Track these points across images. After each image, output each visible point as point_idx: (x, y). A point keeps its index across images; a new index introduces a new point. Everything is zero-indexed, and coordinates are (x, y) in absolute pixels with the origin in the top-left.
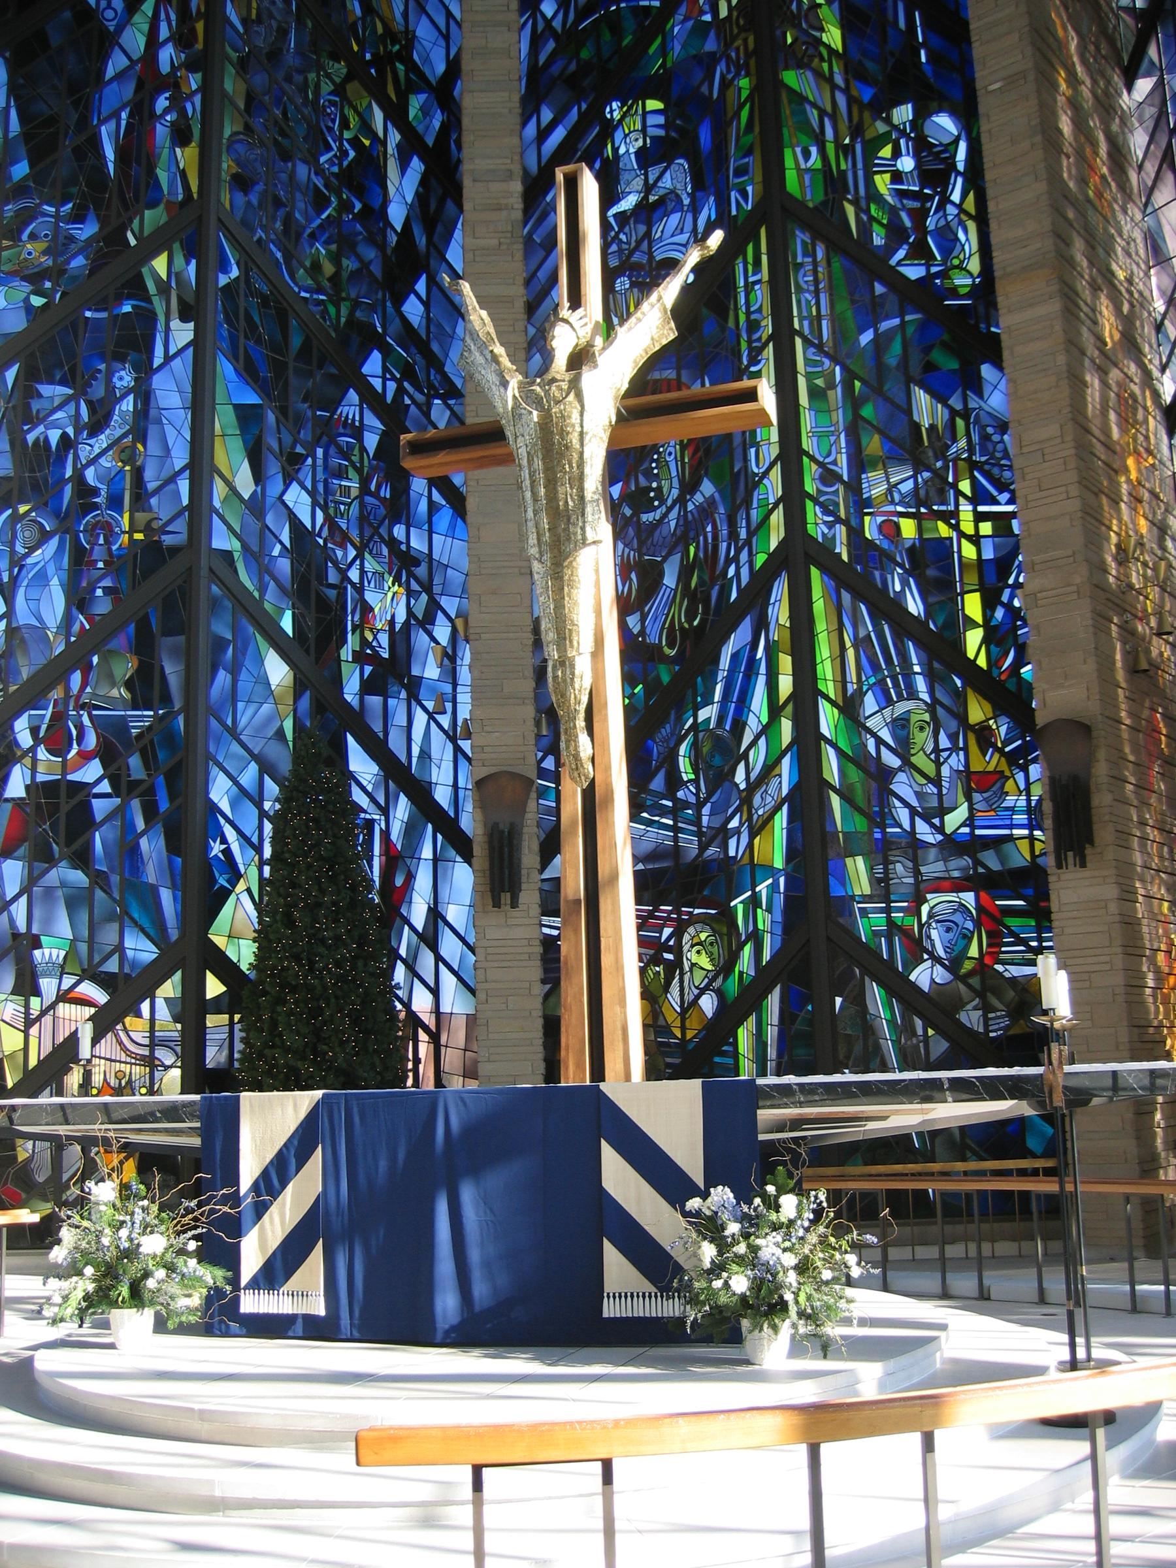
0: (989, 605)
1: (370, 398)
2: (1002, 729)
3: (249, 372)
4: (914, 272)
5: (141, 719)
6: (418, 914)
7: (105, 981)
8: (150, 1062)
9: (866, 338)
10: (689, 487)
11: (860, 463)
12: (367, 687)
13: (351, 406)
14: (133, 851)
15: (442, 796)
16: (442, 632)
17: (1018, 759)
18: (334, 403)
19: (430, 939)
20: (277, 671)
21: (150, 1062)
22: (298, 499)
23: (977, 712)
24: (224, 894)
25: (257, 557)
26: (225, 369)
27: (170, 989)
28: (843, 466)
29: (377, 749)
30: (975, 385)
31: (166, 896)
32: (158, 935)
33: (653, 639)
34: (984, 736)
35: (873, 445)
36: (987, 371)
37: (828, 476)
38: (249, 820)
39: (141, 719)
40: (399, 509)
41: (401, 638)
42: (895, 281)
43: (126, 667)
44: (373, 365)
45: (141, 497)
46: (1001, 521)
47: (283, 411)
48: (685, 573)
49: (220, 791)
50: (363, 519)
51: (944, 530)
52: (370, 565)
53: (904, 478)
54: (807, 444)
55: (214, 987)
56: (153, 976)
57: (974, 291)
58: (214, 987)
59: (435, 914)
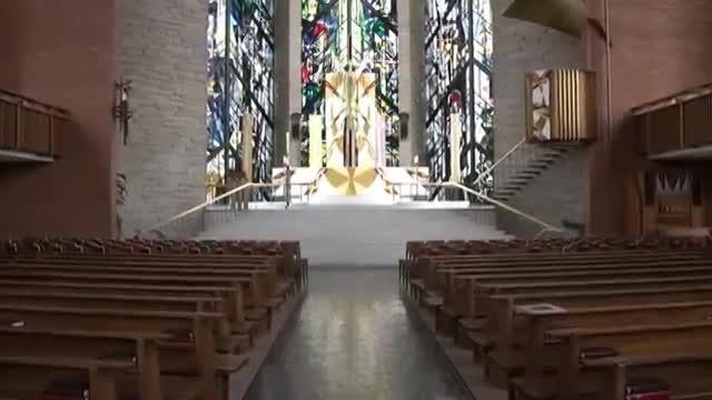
0: (387, 81)
1: (256, 21)
2: (387, 108)
3: (235, 17)
4: (377, 8)
5: (216, 95)
6: (263, 139)
7: (209, 150)
8: (219, 168)
9: (366, 22)
10: (326, 49)
11: (363, 50)
12: (255, 88)
13: (252, 24)
14: (214, 123)
15: (267, 112)
16: (267, 74)
17: (391, 114)
18: (249, 24)
19: (264, 144)
20: (240, 86)
21: (219, 168)
22: (243, 46)
23: (383, 104)
24: (231, 133)
25: (237, 59)
26: (231, 17)
27: (222, 152)
28: (360, 50)
29: (256, 102)
30: (387, 34)
31: (222, 134)
32: (220, 141)
33: (316, 81)
34: (384, 110)
35: (366, 46)
36: (390, 32)
37: (357, 52)
38: (235, 117)
39: (216, 95)
40: (260, 47)
41: (260, 77)
42: (373, 10)
43: (213, 84)
44: (256, 14)
45: (215, 46)
46: (391, 65)
47: (242, 28)
48: (324, 68)
49: (231, 112)
50: (255, 50)
51: (378, 65)
52: (256, 61)
53: (372, 53)
54: (353, 44)
55: (230, 153)
56: (218, 150)
57: (390, 14)
58: (230, 153)
59: (265, 138)
